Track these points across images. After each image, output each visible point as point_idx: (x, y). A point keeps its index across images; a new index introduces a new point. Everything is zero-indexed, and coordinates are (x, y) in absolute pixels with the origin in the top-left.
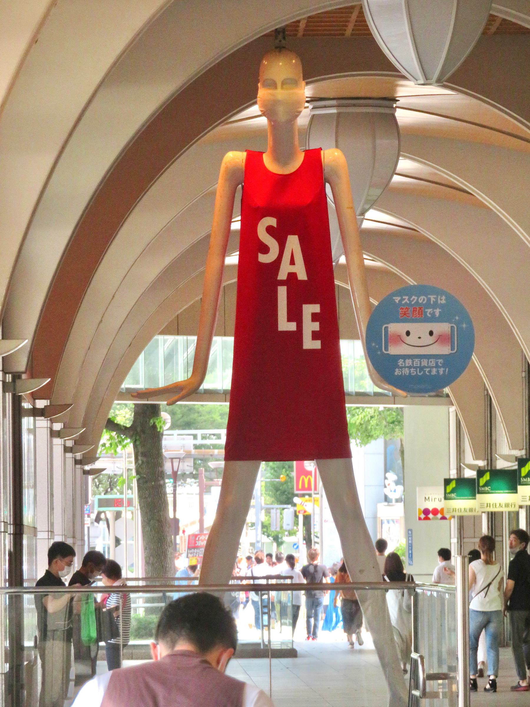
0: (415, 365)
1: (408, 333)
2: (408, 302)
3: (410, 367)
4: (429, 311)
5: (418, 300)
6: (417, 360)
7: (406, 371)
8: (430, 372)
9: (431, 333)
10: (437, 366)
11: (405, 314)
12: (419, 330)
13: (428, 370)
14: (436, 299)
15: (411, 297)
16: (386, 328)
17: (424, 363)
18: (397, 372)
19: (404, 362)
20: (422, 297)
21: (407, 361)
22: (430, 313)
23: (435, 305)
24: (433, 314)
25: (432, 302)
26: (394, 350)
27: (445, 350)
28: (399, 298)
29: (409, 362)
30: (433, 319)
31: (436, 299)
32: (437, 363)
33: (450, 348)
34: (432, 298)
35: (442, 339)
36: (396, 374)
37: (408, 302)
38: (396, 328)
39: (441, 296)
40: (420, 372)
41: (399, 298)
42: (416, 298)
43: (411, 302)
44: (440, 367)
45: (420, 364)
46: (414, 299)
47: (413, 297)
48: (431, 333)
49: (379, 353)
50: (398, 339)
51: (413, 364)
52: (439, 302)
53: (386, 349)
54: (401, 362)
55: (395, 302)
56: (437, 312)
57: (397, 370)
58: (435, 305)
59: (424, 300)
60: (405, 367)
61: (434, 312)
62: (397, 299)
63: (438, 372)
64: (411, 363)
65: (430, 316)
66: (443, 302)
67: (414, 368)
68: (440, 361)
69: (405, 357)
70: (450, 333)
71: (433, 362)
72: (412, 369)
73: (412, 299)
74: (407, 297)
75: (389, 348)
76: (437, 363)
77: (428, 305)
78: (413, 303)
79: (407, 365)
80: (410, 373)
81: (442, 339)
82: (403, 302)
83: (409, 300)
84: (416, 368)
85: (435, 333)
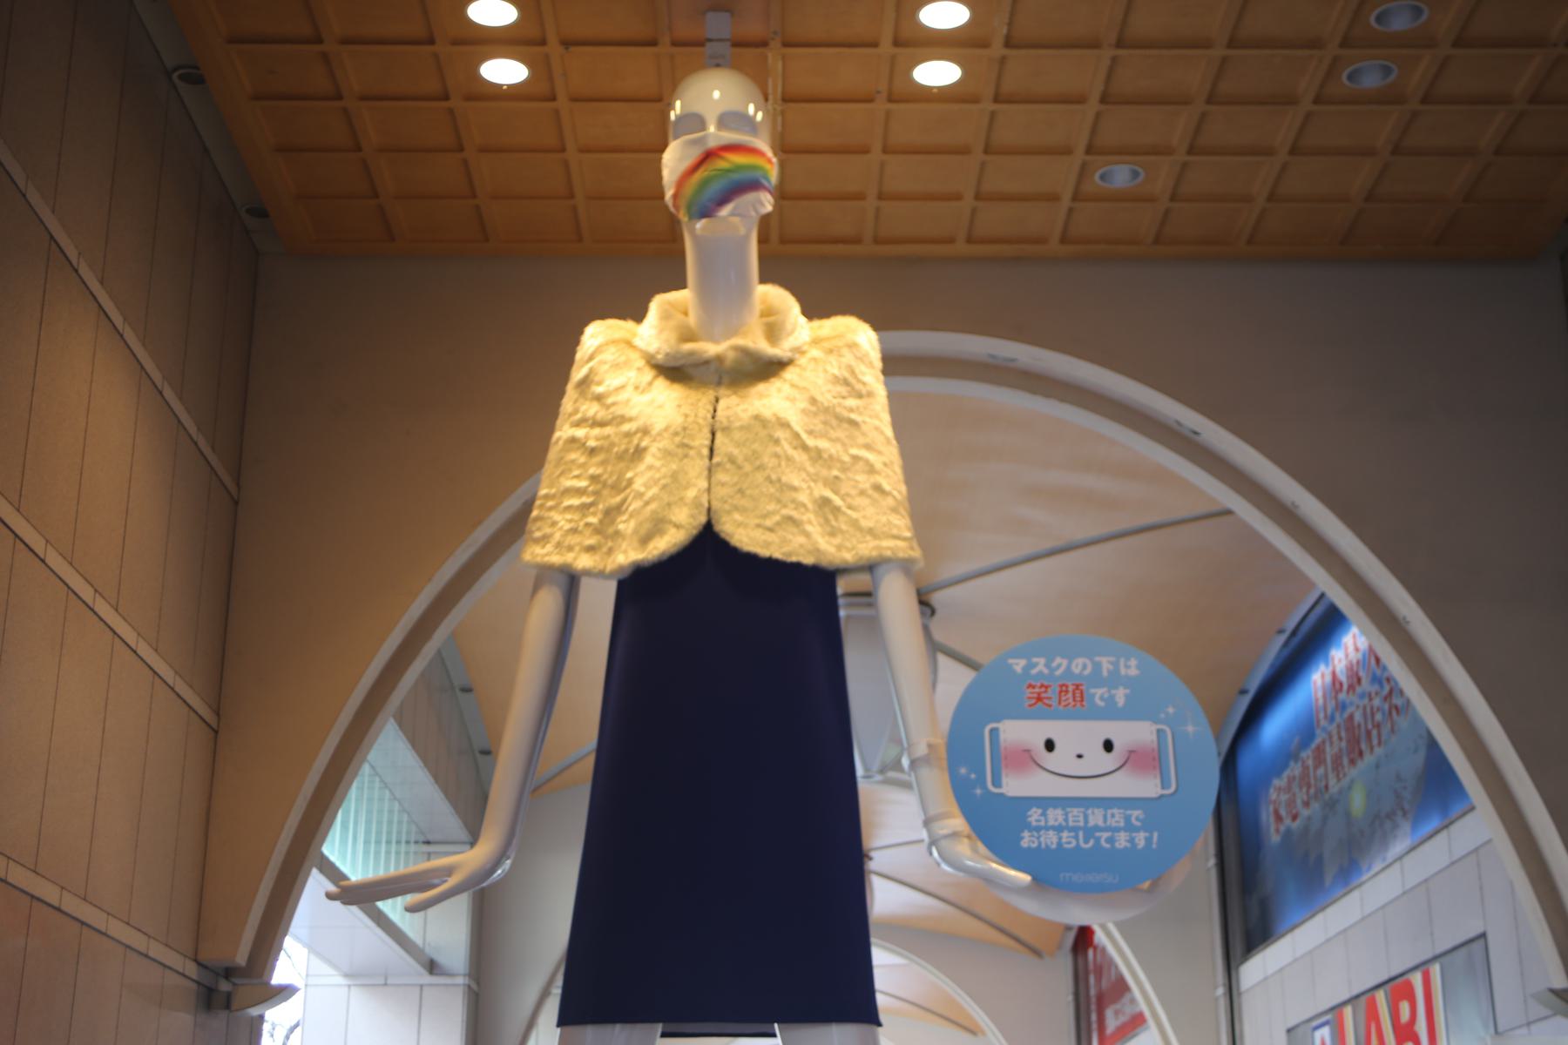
0: (1071, 824)
1: (1050, 745)
2: (1046, 671)
3: (1059, 829)
4: (1099, 692)
5: (1068, 668)
6: (1075, 811)
7: (1050, 839)
8: (1111, 840)
9: (1108, 746)
10: (1129, 827)
11: (1039, 699)
12: (1078, 737)
13: (1105, 835)
14: (1116, 664)
15: (1053, 660)
16: (994, 732)
17: (1096, 817)
18: (1027, 841)
19: (1044, 814)
20: (1080, 661)
21: (1051, 813)
22: (1102, 699)
23: (1114, 680)
24: (1111, 701)
25: (1105, 673)
26: (1015, 785)
27: (1148, 787)
28: (1023, 662)
29: (1056, 816)
30: (1110, 712)
31: (1116, 664)
32: (1127, 819)
33: (1158, 781)
34: (1106, 663)
35: (1137, 760)
36: (1025, 844)
37: (1046, 671)
38: (1020, 732)
39: (1128, 659)
40: (1086, 842)
41: (1023, 662)
42: (1065, 663)
43: (1052, 670)
44: (1137, 830)
45: (1086, 821)
46: (1059, 666)
47: (1058, 660)
48: (1108, 746)
49: (978, 791)
50: (1023, 759)
51: (1066, 820)
52: (1123, 671)
53: (997, 782)
54: (1034, 815)
55: (1014, 672)
56: (1120, 695)
57: (1026, 834)
58: (1114, 680)
59: (1085, 667)
60: (1047, 828)
61: (1112, 697)
62: (1019, 665)
63: (1132, 840)
64: (1061, 819)
65: (1102, 704)
66: (1133, 672)
67: (1071, 829)
68: (1136, 813)
69: (1045, 803)
70: (1155, 745)
71: (1117, 817)
72: (1065, 834)
73: (1054, 665)
74: (1042, 661)
75: (1005, 780)
76: (1127, 819)
77: (1096, 679)
78: (1058, 673)
79: (1051, 823)
80: (1059, 844)
81: (1137, 760)
82: (1034, 672)
83: (1047, 666)
84: (1071, 829)
85: (1116, 744)
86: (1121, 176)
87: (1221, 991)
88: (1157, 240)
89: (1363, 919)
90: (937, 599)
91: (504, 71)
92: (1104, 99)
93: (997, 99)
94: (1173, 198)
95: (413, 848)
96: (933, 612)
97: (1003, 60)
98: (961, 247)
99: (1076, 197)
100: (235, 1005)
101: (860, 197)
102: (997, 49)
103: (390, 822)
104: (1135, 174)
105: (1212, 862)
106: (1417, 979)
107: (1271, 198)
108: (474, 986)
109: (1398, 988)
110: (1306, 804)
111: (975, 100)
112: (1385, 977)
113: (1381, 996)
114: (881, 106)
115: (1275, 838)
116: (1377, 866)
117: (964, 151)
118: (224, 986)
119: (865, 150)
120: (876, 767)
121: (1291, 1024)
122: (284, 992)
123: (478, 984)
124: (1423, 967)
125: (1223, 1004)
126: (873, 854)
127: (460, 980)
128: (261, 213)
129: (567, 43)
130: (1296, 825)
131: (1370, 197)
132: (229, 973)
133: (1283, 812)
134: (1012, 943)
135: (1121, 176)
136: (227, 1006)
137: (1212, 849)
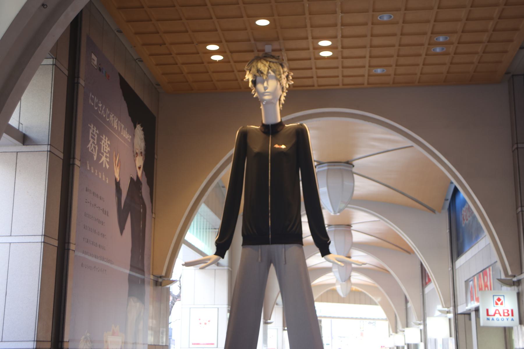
86: (379, 71)
87: (450, 269)
88: (394, 83)
89: (479, 252)
90: (354, 163)
91: (217, 58)
92: (370, 57)
93: (343, 58)
94: (395, 75)
95: (211, 230)
96: (353, 166)
97: (342, 51)
98: (341, 86)
99: (369, 75)
100: (163, 285)
101: (312, 77)
102: (340, 49)
103: (203, 224)
104: (384, 71)
105: (448, 231)
106: (488, 270)
107: (421, 74)
108: (230, 269)
109: (484, 271)
110: (469, 217)
111: (337, 58)
112: (482, 269)
113: (481, 274)
114: (313, 61)
115: (463, 225)
116: (483, 236)
117: (337, 68)
118: (160, 280)
119: (311, 69)
120: (337, 211)
121: (466, 279)
122: (173, 282)
123: (231, 268)
124: (488, 267)
125: (451, 273)
126: (352, 225)
127: (226, 268)
128: (158, 85)
129: (232, 52)
130: (467, 222)
131: (448, 72)
132: (161, 277)
133: (465, 218)
134: (400, 250)
135: (379, 71)
136: (161, 285)
137: (448, 227)
